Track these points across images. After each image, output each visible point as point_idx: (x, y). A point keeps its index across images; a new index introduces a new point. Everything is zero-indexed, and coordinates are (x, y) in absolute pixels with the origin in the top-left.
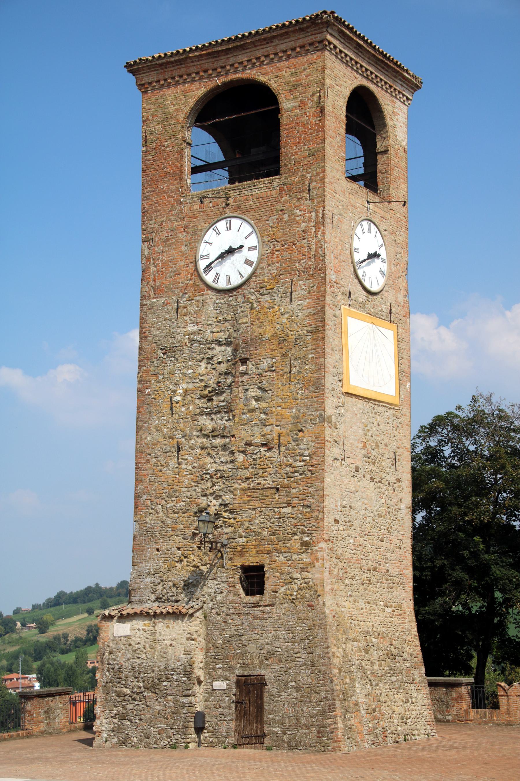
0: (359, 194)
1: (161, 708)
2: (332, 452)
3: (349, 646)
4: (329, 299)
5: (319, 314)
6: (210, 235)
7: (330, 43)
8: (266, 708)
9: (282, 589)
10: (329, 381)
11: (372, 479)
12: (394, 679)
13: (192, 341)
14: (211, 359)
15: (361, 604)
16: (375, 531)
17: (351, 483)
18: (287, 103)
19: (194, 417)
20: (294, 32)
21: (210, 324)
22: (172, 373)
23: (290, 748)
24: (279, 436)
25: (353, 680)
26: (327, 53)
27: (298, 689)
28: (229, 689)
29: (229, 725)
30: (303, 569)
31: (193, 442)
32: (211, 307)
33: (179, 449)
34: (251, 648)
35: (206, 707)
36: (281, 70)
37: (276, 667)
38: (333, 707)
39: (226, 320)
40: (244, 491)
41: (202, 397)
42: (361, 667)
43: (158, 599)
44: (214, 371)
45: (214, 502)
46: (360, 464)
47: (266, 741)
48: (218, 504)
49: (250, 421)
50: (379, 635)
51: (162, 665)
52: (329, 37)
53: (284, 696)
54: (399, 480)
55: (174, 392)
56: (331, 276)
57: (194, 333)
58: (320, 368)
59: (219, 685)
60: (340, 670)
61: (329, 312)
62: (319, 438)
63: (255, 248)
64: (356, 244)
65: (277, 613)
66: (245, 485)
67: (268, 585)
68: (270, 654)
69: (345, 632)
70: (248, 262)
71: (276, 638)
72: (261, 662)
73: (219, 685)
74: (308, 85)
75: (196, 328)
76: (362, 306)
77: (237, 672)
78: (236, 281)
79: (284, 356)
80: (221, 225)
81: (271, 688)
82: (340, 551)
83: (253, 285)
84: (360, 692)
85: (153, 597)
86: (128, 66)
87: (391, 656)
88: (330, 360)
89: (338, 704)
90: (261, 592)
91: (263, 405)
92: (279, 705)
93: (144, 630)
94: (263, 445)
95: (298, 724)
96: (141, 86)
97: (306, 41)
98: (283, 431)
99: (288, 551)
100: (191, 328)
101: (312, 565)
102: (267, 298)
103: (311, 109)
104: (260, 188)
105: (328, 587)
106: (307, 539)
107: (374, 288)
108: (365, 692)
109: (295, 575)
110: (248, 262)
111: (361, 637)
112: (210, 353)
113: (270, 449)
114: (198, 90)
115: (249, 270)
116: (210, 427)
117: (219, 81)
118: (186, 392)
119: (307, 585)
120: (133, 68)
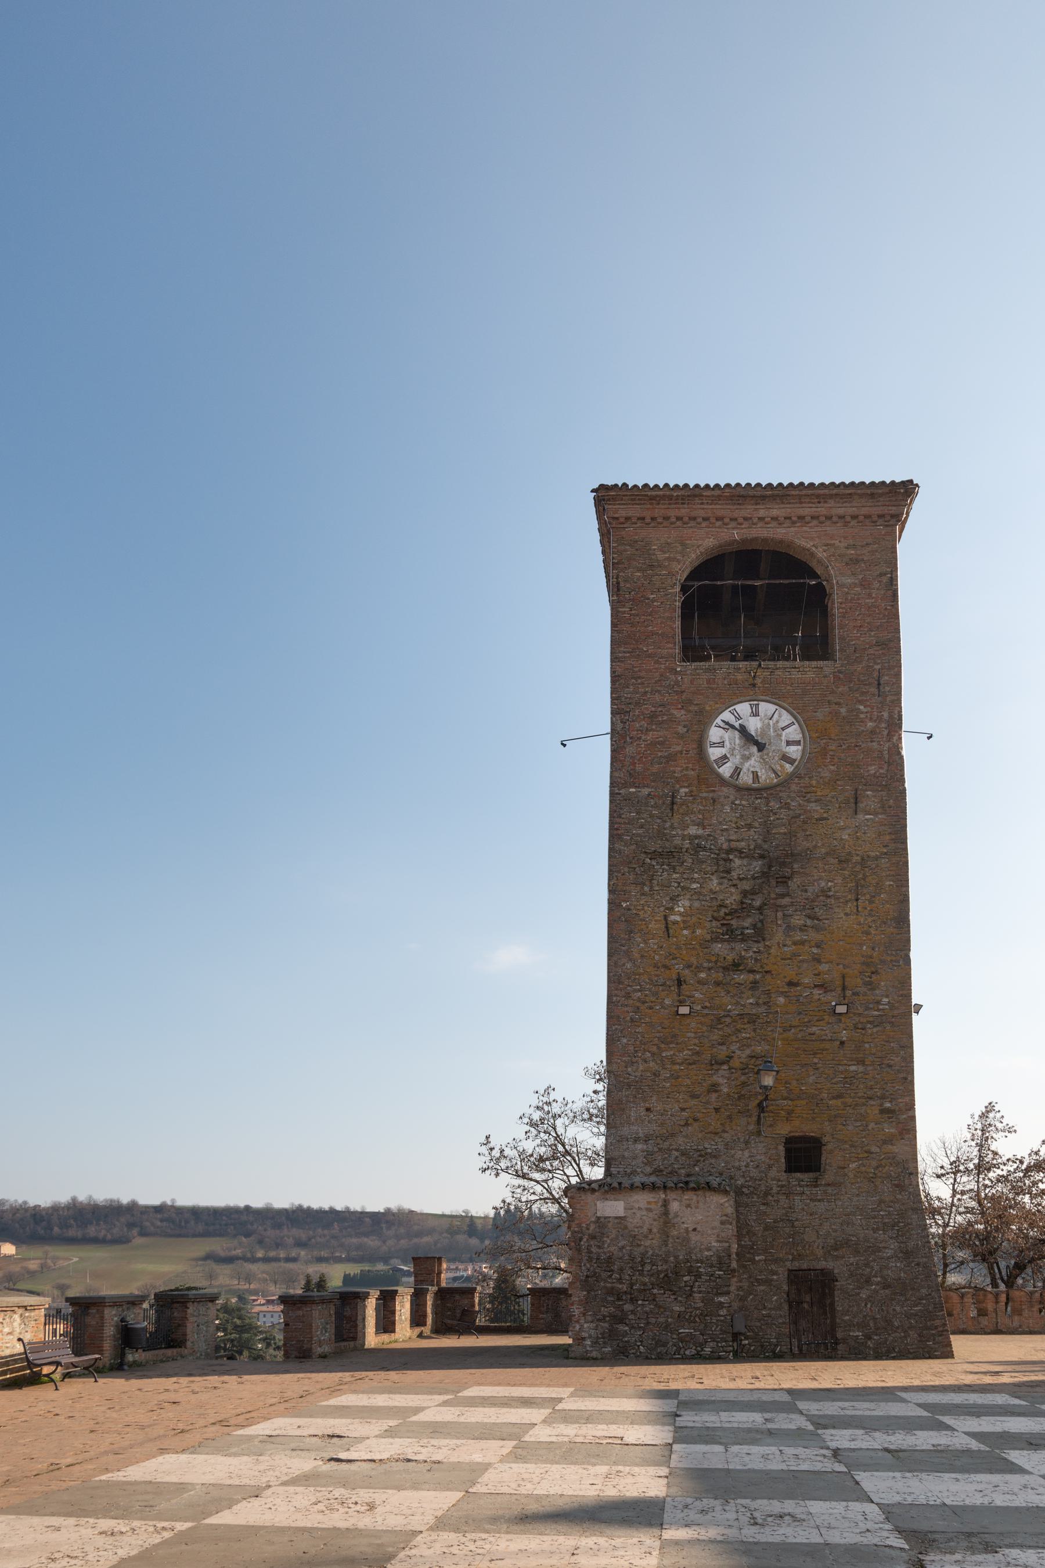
1: (683, 1309)
19: (705, 944)
21: (726, 830)
31: (703, 975)
32: (727, 809)
44: (733, 890)
45: (738, 1052)
48: (744, 1056)
63: (798, 743)
93: (649, 1210)
114: (704, 541)
116: (730, 958)
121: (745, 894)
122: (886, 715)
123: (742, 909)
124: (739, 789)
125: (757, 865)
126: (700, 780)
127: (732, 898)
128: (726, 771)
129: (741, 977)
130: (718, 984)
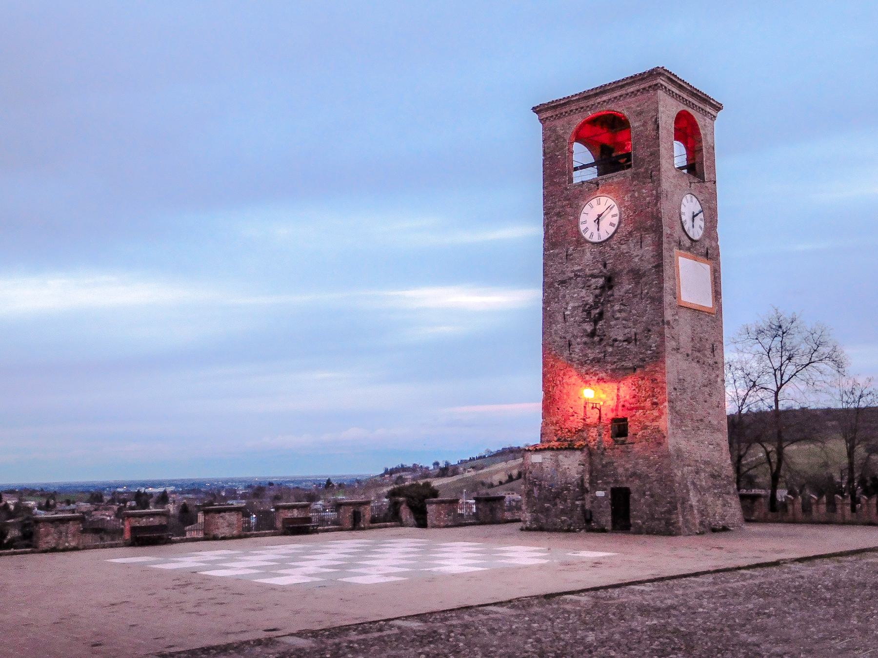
0: (685, 179)
2: (670, 344)
3: (685, 469)
4: (665, 246)
5: (659, 255)
6: (587, 209)
7: (662, 85)
8: (631, 508)
9: (640, 433)
10: (668, 298)
11: (698, 362)
12: (716, 491)
13: (576, 275)
14: (589, 286)
15: (693, 442)
16: (700, 395)
17: (684, 365)
18: (635, 124)
20: (639, 80)
22: (564, 296)
23: (648, 533)
24: (636, 334)
25: (688, 491)
26: (659, 91)
27: (652, 496)
28: (606, 496)
29: (606, 519)
30: (653, 420)
31: (578, 340)
32: (588, 254)
33: (570, 345)
34: (620, 470)
35: (593, 507)
36: (630, 103)
37: (637, 482)
38: (676, 508)
39: (598, 261)
40: (613, 370)
41: (584, 311)
42: (693, 484)
43: (559, 440)
46: (690, 352)
47: (632, 528)
49: (615, 325)
50: (706, 463)
51: (563, 481)
52: (662, 82)
53: (642, 501)
54: (716, 363)
55: (566, 309)
56: (666, 230)
57: (579, 271)
58: (661, 289)
59: (600, 494)
60: (680, 484)
61: (665, 253)
62: (662, 335)
64: (683, 209)
65: (637, 448)
66: (614, 367)
67: (631, 431)
68: (634, 474)
69: (682, 460)
70: (612, 224)
71: (637, 464)
72: (627, 479)
73: (600, 494)
74: (649, 112)
75: (579, 268)
76: (689, 249)
77: (612, 486)
78: (605, 237)
79: (637, 283)
80: (594, 202)
81: (634, 496)
82: (678, 408)
83: (615, 238)
84: (693, 499)
85: (556, 439)
86: (534, 108)
87: (713, 476)
88: (667, 285)
89: (679, 506)
90: (626, 435)
91: (624, 315)
92: (639, 506)
94: (624, 341)
95: (653, 518)
96: (541, 120)
97: (647, 85)
98: (638, 331)
99: (643, 408)
100: (576, 268)
101: (659, 417)
102: (623, 247)
103: (650, 126)
104: (617, 177)
105: (670, 432)
106: (656, 400)
107: (696, 238)
108: (696, 499)
109: (648, 423)
110: (612, 224)
111: (693, 463)
112: (589, 284)
113: (629, 343)
114: (578, 120)
115: (613, 229)
117: (590, 114)
118: (574, 308)
119: (657, 430)
120: (537, 110)
121: (596, 296)
122: (654, 192)
123: (596, 305)
124: (593, 243)
125: (601, 281)
126: (578, 241)
127: (590, 300)
128: (587, 236)
129: (596, 339)
130: (585, 343)
